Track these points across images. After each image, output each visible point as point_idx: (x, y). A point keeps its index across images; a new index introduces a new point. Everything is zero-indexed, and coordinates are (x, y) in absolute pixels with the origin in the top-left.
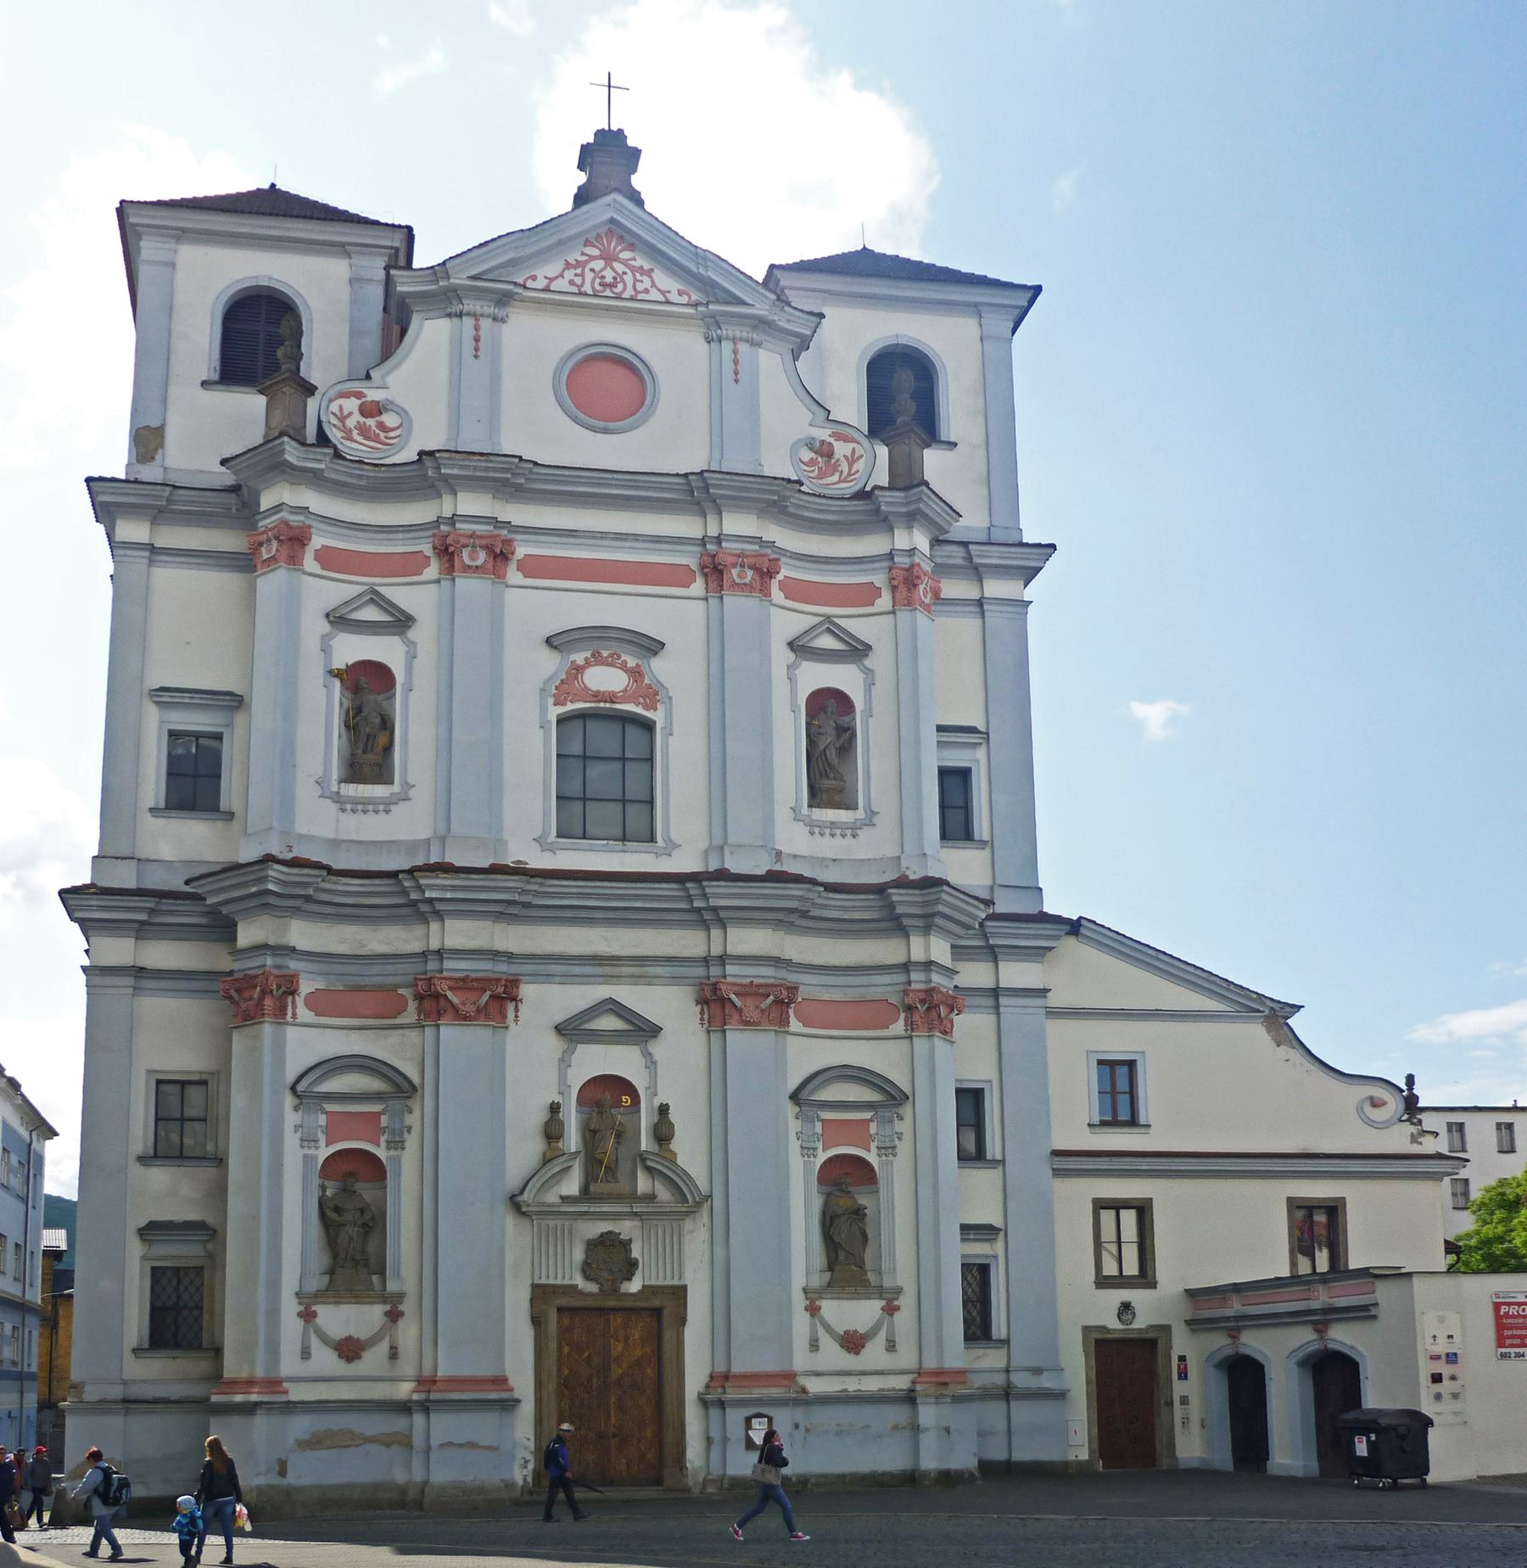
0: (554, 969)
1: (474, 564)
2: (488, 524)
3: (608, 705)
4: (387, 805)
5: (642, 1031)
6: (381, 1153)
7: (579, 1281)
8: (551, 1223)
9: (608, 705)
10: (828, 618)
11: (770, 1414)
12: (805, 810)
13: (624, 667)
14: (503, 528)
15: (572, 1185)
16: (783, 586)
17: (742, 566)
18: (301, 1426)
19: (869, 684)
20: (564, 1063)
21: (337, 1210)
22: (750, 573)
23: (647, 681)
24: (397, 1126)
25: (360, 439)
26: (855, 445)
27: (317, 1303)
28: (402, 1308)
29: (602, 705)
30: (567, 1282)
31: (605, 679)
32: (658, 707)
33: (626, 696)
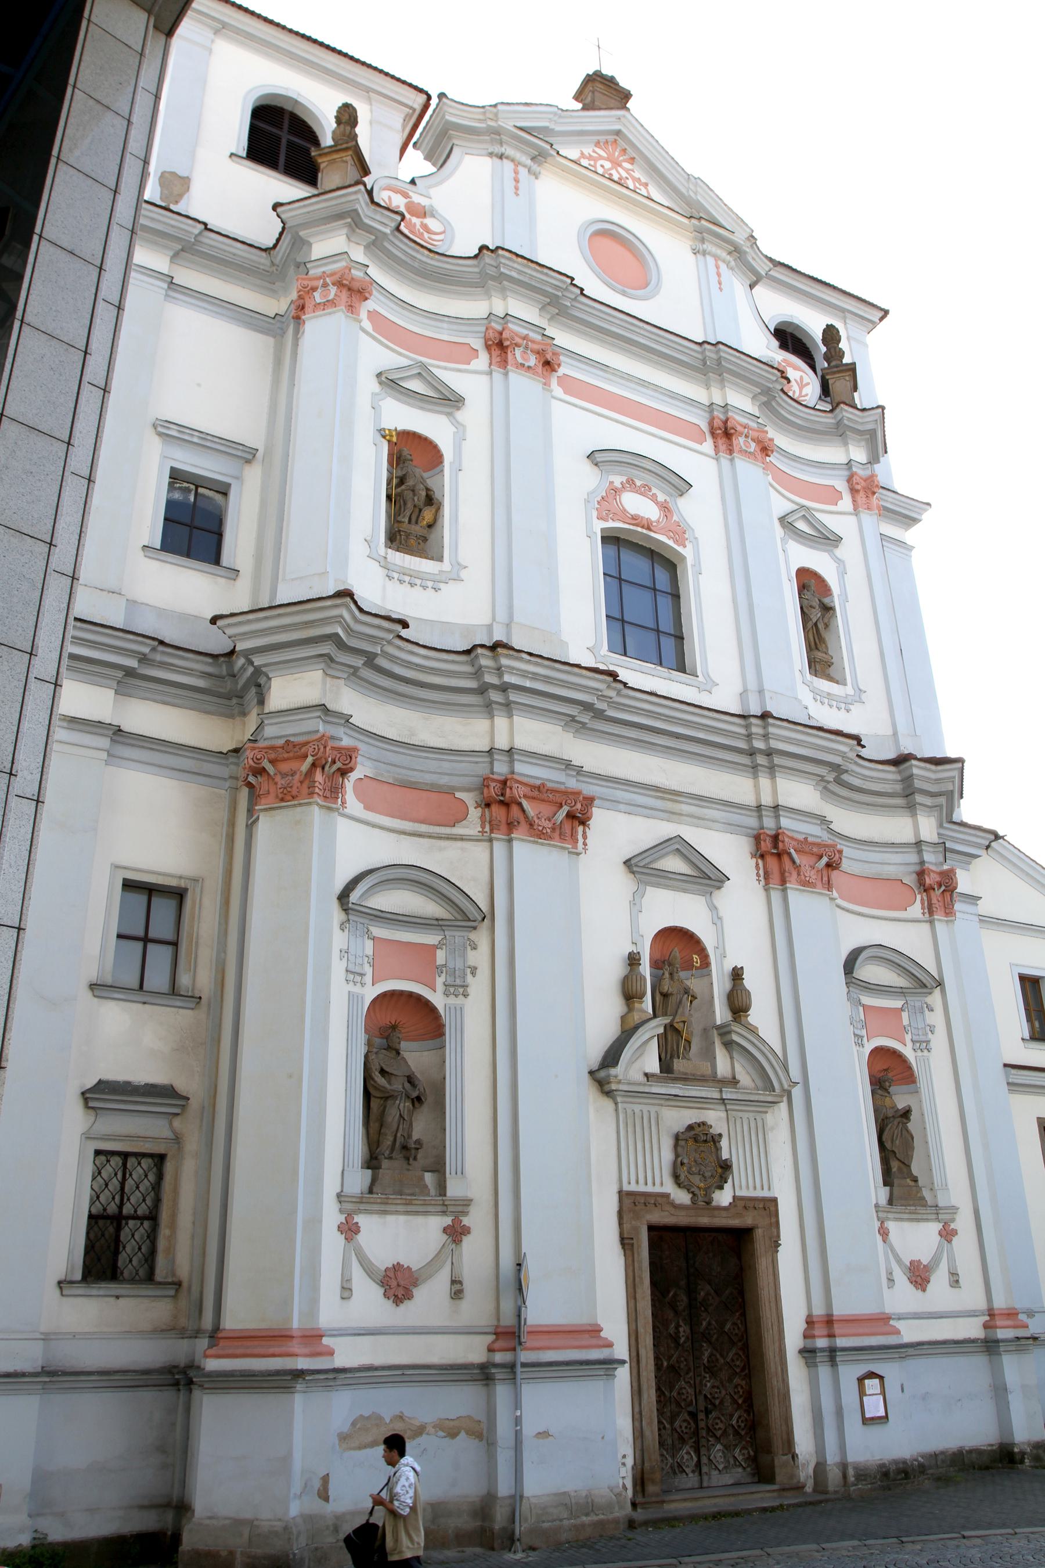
3: (645, 531)
4: (436, 583)
6: (437, 999)
7: (669, 1187)
8: (637, 1108)
9: (645, 531)
13: (654, 498)
17: (746, 436)
19: (842, 572)
22: (753, 445)
23: (675, 518)
24: (459, 965)
26: (801, 373)
27: (359, 1211)
28: (466, 1221)
29: (639, 529)
30: (657, 1189)
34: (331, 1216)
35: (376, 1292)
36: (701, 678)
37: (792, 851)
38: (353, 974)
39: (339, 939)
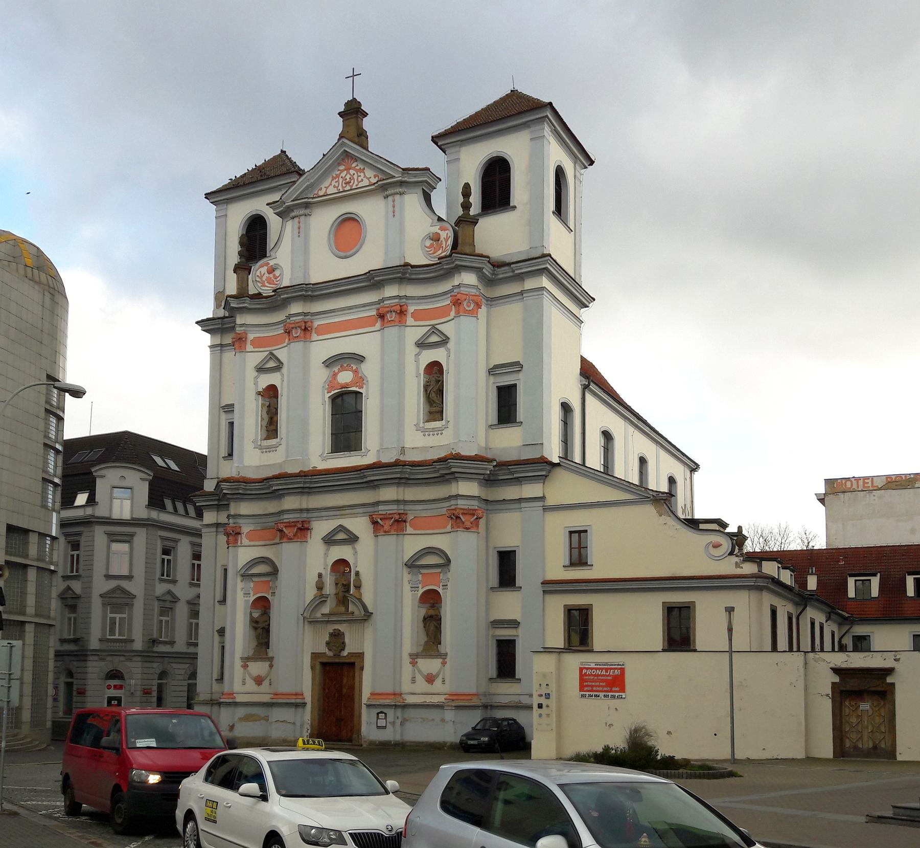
0: (324, 514)
1: (297, 335)
2: (302, 315)
3: (346, 389)
5: (352, 539)
7: (327, 651)
9: (346, 389)
10: (433, 326)
11: (384, 711)
12: (422, 425)
14: (308, 315)
15: (326, 609)
16: (413, 315)
18: (241, 712)
20: (326, 555)
21: (257, 622)
23: (360, 375)
25: (267, 285)
29: (343, 389)
31: (345, 377)
32: (364, 386)
33: (353, 383)
34: (238, 663)
35: (253, 683)
36: (363, 450)
37: (379, 520)
38: (247, 594)
39: (240, 585)
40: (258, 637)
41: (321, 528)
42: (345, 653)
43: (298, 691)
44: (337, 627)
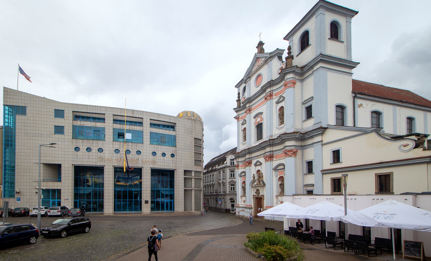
0: (254, 158)
5: (261, 164)
15: (256, 184)
21: (243, 187)
39: (239, 178)
40: (244, 191)
41: (254, 162)
42: (260, 195)
43: (251, 205)
44: (258, 188)
